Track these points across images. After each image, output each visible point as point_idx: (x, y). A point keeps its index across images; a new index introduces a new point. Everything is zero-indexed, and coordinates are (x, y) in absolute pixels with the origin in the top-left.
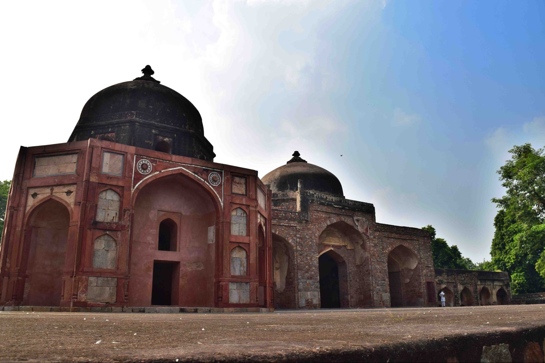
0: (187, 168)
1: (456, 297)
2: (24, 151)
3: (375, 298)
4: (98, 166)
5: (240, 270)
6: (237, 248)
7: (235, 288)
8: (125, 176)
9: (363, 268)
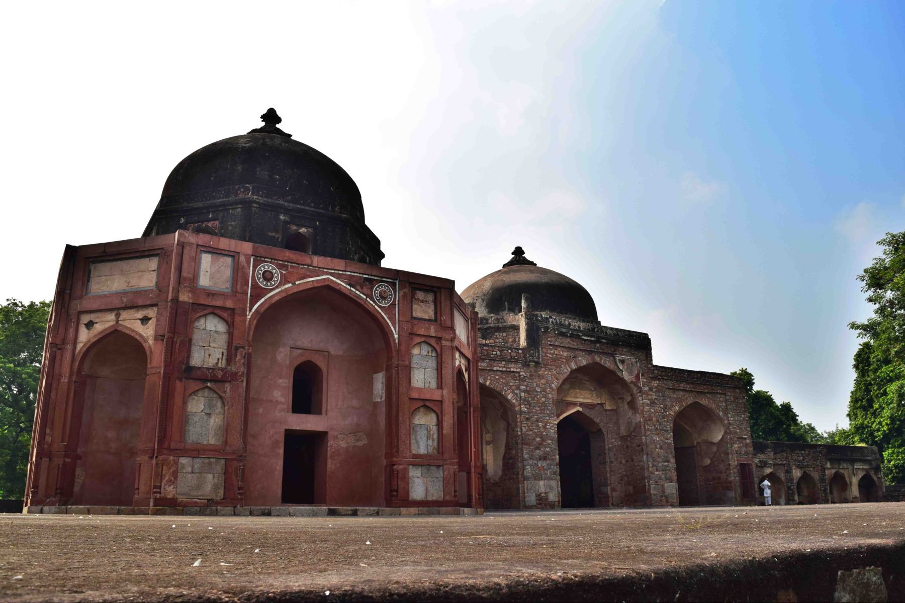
0: (338, 276)
1: (789, 488)
2: (71, 252)
3: (652, 492)
4: (191, 276)
5: (427, 446)
6: (422, 409)
7: (419, 475)
8: (236, 292)
9: (632, 442)
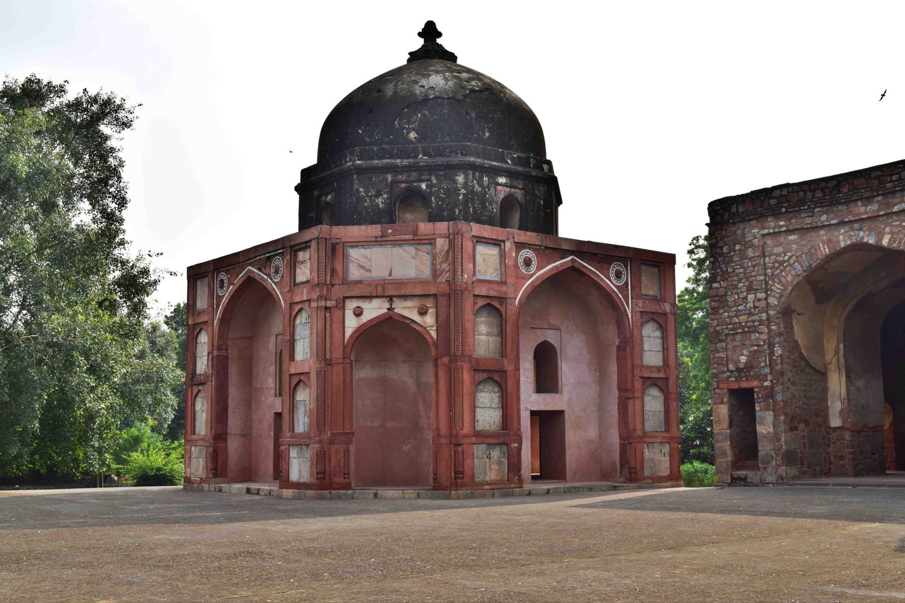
7: (295, 455)
